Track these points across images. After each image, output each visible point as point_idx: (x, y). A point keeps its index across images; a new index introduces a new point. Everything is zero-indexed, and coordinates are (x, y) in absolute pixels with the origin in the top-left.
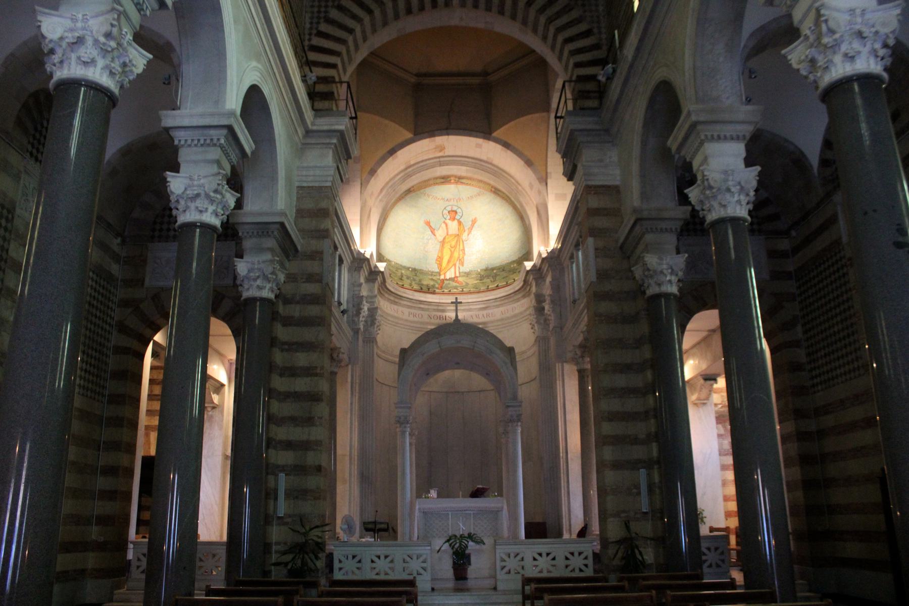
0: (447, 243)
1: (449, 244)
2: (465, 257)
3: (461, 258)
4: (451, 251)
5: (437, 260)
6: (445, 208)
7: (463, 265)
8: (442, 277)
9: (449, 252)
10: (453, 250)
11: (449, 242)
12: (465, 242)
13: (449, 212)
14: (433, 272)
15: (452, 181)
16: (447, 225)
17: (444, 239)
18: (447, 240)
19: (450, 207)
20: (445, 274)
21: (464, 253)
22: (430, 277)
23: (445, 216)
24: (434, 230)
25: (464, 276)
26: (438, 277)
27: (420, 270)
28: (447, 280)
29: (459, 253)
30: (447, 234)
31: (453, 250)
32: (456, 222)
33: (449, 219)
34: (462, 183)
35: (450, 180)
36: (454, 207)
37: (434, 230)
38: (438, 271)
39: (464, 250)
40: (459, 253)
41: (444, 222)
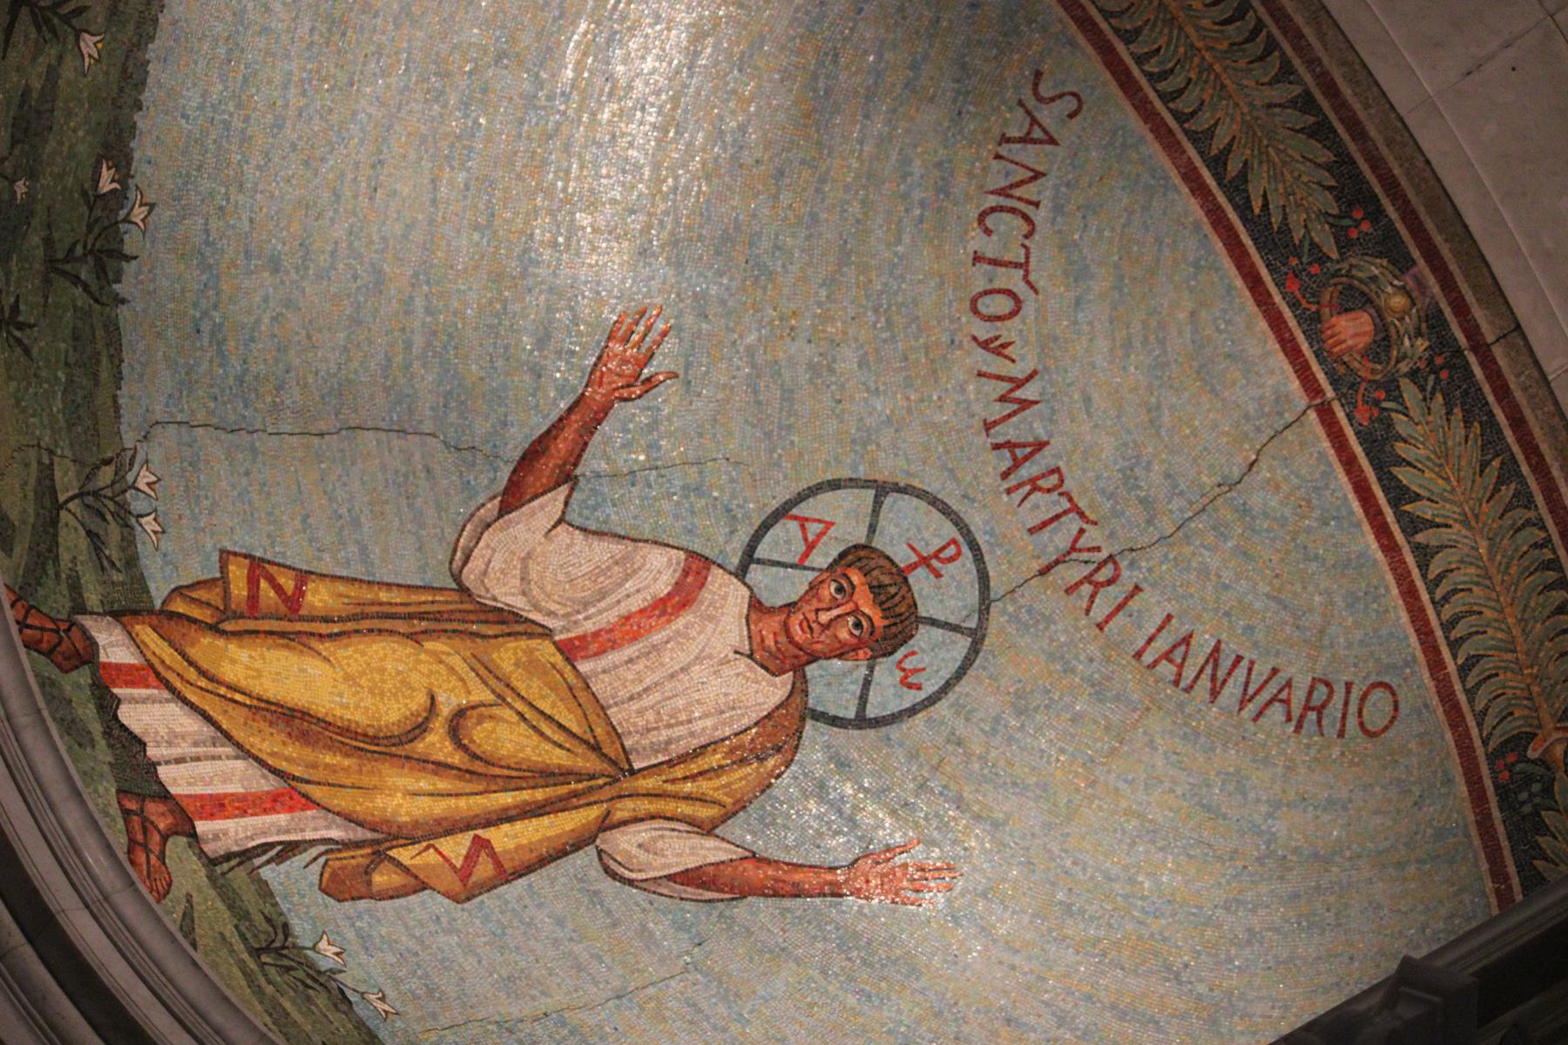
0: (487, 671)
1: (481, 694)
2: (434, 902)
3: (404, 855)
4: (420, 728)
5: (258, 567)
6: (882, 489)
7: (337, 888)
8: (114, 647)
9: (392, 713)
10: (436, 743)
11: (504, 691)
12: (586, 857)
13: (857, 556)
14: (125, 517)
15: (1352, 329)
16: (680, 599)
17: (509, 622)
18: (507, 655)
19: (937, 532)
20: (149, 674)
21: (466, 890)
22: (67, 479)
23: (783, 540)
24: (567, 477)
25: (240, 914)
26: (93, 599)
27: (113, 332)
28: (107, 706)
29: (451, 827)
30: (569, 650)
31: (436, 743)
32: (771, 691)
33: (756, 606)
34: (1380, 443)
35: (1356, 298)
36: (962, 570)
37: (567, 477)
38: (159, 591)
39: (506, 874)
40: (451, 827)
41: (698, 566)
